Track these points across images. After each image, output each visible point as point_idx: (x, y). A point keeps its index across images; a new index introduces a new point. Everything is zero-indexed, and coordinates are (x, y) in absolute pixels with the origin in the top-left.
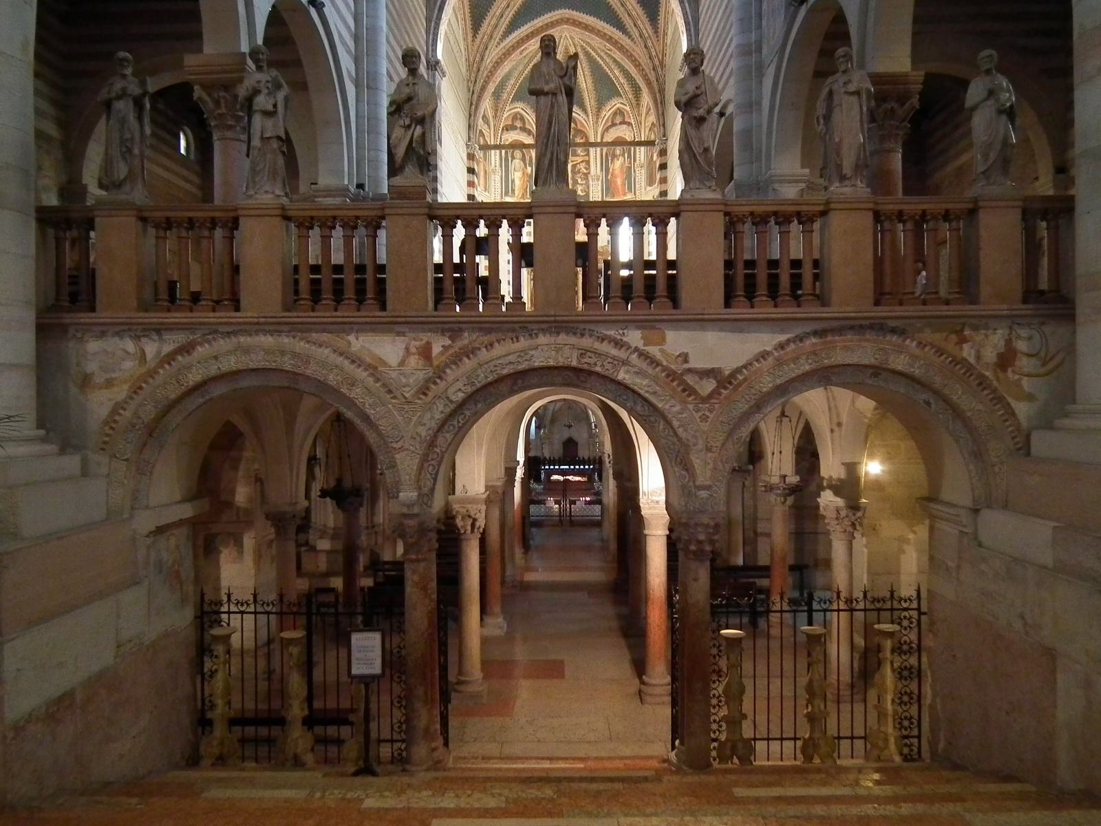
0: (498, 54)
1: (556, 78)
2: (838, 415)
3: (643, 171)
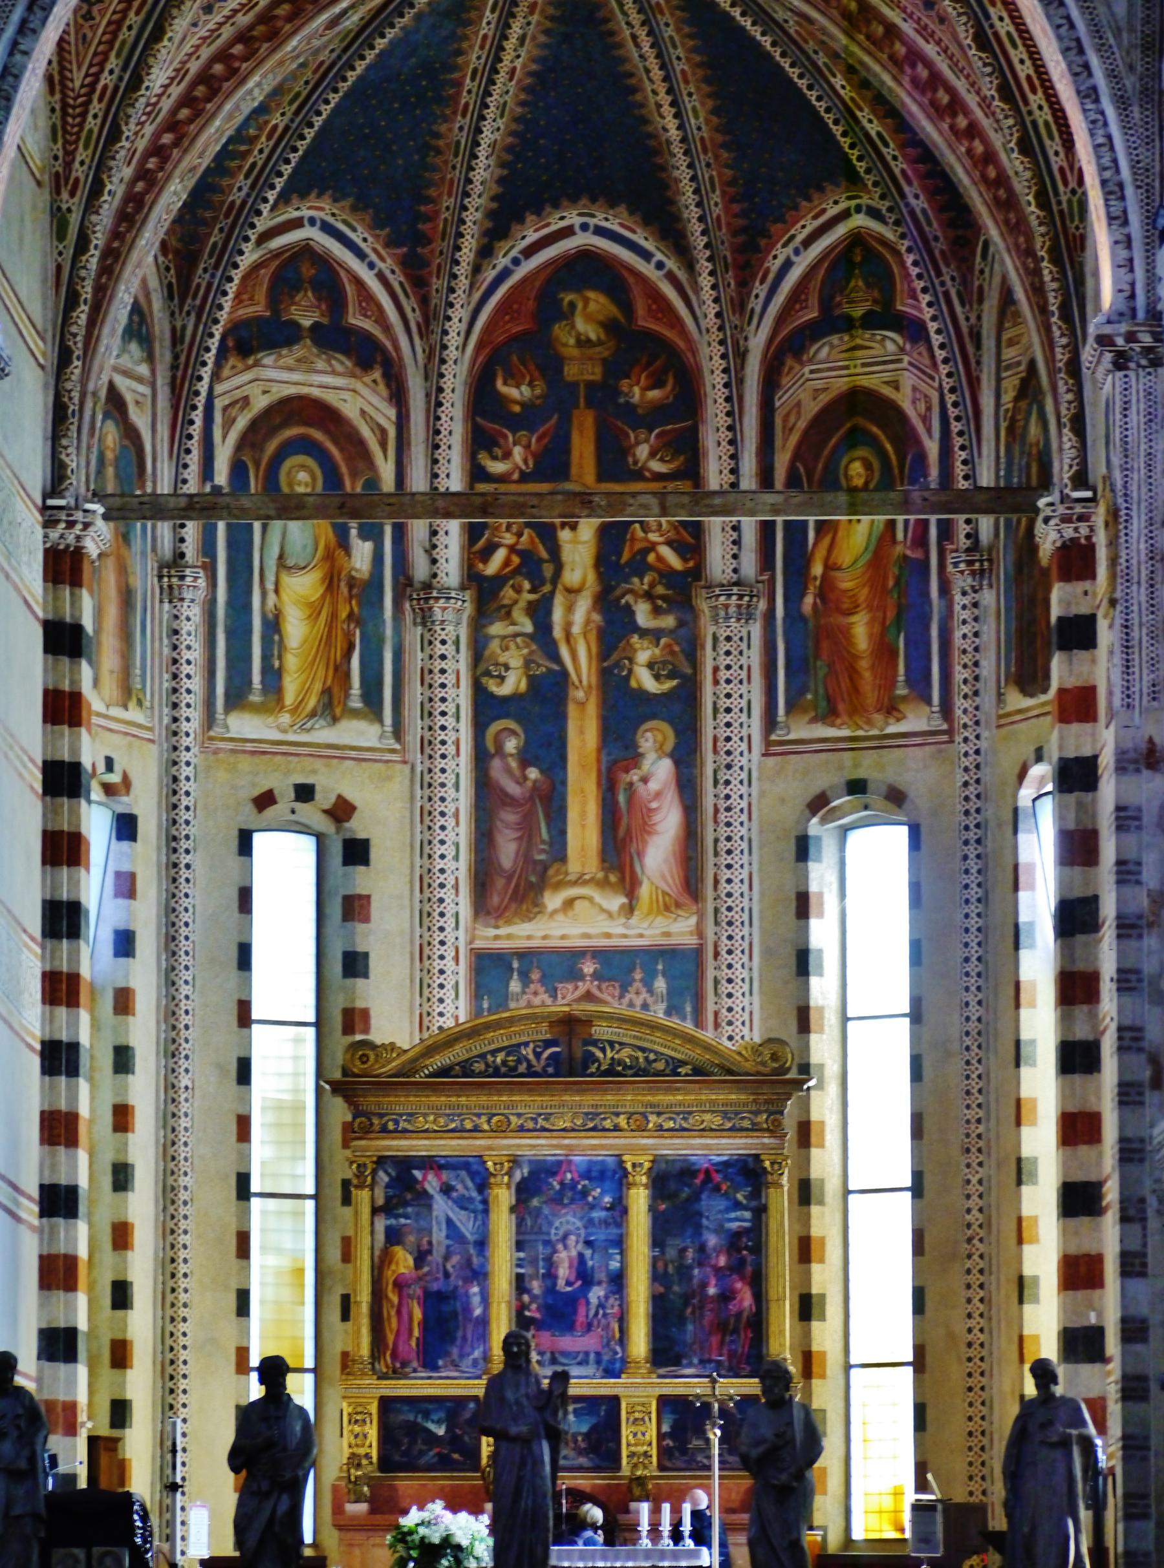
0: (214, 33)
1: (529, 1411)
3: (988, 597)
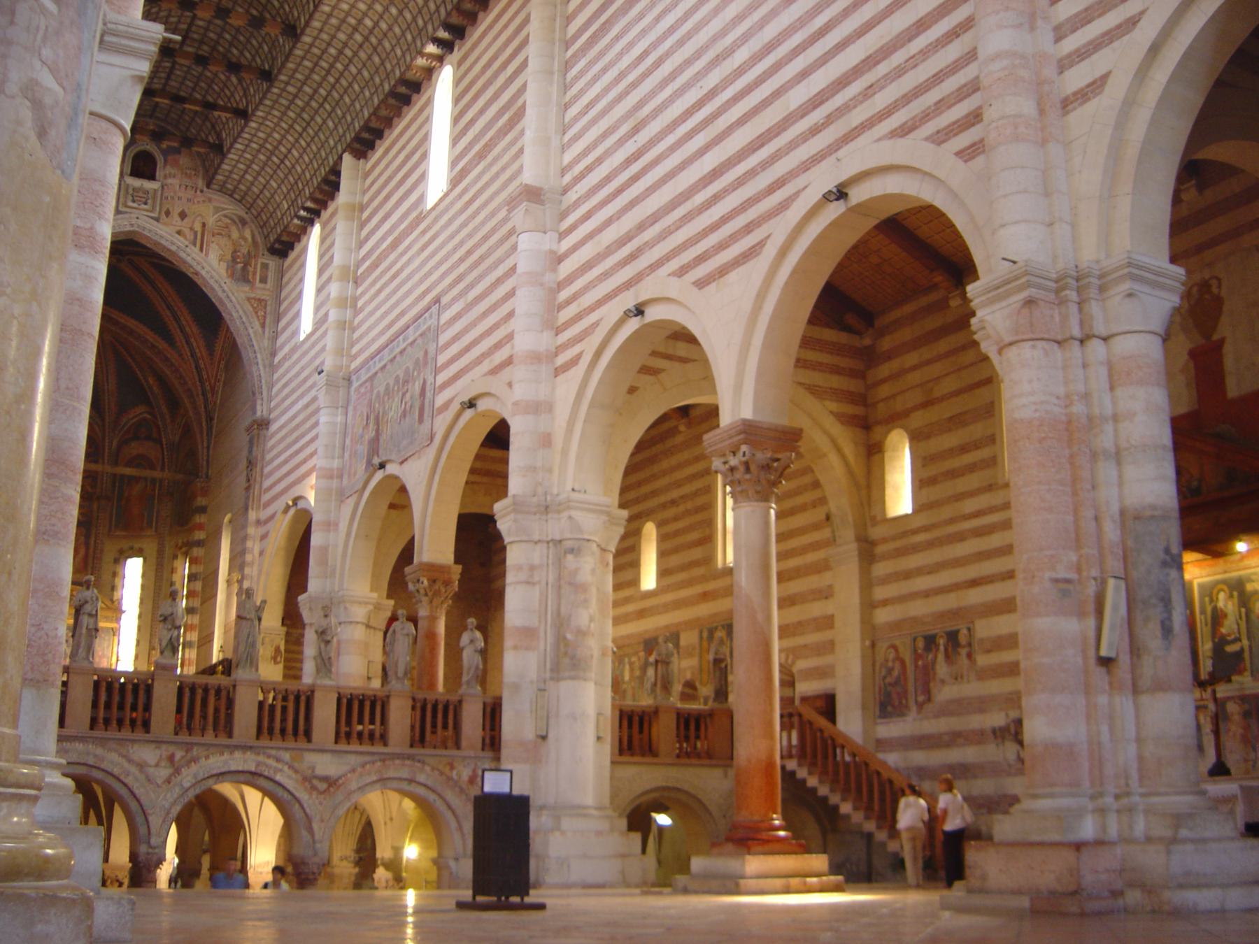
2: (391, 812)
